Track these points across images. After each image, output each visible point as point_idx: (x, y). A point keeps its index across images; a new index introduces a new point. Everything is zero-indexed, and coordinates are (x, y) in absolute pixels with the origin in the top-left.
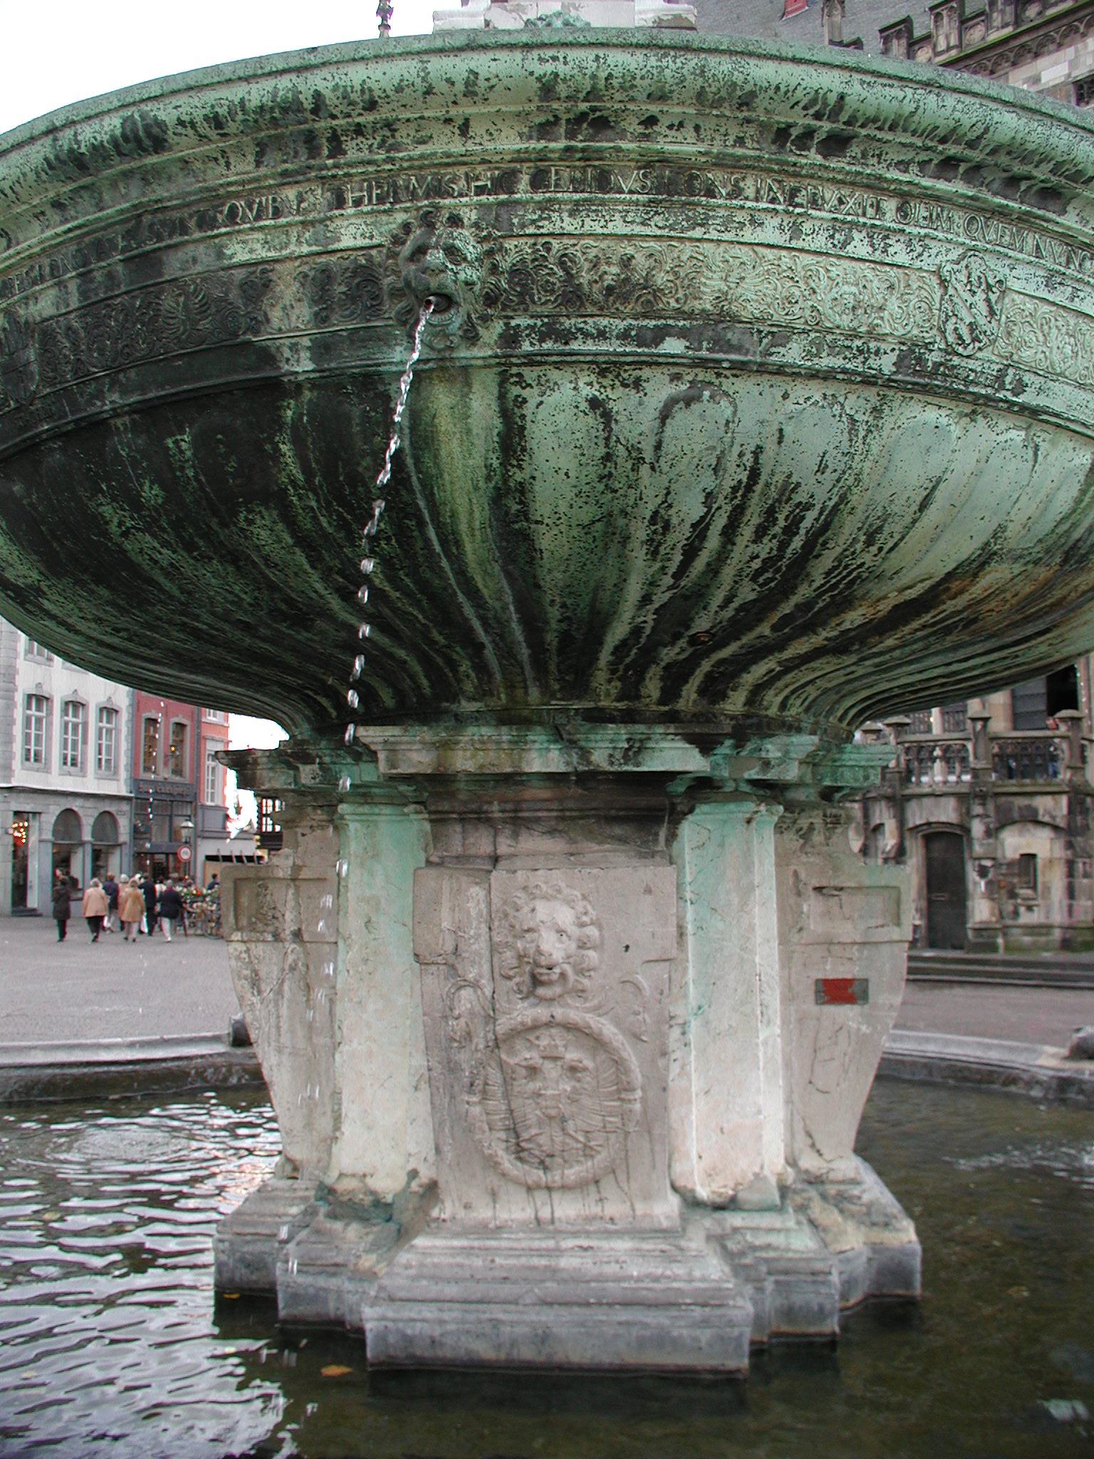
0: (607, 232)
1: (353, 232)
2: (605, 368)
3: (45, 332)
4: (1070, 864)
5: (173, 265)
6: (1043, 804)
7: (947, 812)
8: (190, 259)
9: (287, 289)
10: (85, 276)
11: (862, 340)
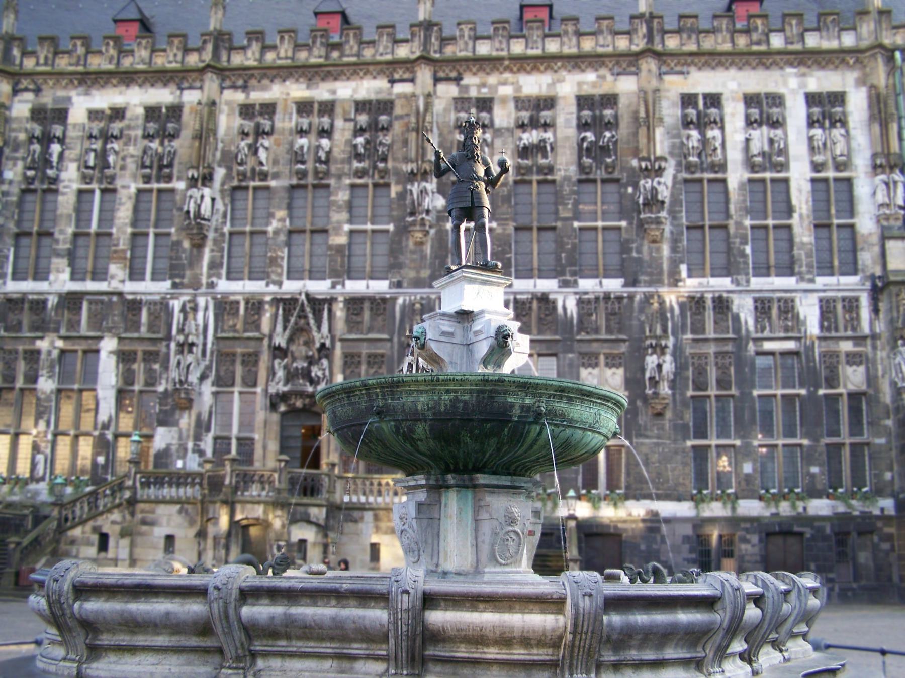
0: (560, 406)
2: (555, 425)
3: (465, 402)
4: (326, 547)
8: (500, 399)
9: (517, 407)
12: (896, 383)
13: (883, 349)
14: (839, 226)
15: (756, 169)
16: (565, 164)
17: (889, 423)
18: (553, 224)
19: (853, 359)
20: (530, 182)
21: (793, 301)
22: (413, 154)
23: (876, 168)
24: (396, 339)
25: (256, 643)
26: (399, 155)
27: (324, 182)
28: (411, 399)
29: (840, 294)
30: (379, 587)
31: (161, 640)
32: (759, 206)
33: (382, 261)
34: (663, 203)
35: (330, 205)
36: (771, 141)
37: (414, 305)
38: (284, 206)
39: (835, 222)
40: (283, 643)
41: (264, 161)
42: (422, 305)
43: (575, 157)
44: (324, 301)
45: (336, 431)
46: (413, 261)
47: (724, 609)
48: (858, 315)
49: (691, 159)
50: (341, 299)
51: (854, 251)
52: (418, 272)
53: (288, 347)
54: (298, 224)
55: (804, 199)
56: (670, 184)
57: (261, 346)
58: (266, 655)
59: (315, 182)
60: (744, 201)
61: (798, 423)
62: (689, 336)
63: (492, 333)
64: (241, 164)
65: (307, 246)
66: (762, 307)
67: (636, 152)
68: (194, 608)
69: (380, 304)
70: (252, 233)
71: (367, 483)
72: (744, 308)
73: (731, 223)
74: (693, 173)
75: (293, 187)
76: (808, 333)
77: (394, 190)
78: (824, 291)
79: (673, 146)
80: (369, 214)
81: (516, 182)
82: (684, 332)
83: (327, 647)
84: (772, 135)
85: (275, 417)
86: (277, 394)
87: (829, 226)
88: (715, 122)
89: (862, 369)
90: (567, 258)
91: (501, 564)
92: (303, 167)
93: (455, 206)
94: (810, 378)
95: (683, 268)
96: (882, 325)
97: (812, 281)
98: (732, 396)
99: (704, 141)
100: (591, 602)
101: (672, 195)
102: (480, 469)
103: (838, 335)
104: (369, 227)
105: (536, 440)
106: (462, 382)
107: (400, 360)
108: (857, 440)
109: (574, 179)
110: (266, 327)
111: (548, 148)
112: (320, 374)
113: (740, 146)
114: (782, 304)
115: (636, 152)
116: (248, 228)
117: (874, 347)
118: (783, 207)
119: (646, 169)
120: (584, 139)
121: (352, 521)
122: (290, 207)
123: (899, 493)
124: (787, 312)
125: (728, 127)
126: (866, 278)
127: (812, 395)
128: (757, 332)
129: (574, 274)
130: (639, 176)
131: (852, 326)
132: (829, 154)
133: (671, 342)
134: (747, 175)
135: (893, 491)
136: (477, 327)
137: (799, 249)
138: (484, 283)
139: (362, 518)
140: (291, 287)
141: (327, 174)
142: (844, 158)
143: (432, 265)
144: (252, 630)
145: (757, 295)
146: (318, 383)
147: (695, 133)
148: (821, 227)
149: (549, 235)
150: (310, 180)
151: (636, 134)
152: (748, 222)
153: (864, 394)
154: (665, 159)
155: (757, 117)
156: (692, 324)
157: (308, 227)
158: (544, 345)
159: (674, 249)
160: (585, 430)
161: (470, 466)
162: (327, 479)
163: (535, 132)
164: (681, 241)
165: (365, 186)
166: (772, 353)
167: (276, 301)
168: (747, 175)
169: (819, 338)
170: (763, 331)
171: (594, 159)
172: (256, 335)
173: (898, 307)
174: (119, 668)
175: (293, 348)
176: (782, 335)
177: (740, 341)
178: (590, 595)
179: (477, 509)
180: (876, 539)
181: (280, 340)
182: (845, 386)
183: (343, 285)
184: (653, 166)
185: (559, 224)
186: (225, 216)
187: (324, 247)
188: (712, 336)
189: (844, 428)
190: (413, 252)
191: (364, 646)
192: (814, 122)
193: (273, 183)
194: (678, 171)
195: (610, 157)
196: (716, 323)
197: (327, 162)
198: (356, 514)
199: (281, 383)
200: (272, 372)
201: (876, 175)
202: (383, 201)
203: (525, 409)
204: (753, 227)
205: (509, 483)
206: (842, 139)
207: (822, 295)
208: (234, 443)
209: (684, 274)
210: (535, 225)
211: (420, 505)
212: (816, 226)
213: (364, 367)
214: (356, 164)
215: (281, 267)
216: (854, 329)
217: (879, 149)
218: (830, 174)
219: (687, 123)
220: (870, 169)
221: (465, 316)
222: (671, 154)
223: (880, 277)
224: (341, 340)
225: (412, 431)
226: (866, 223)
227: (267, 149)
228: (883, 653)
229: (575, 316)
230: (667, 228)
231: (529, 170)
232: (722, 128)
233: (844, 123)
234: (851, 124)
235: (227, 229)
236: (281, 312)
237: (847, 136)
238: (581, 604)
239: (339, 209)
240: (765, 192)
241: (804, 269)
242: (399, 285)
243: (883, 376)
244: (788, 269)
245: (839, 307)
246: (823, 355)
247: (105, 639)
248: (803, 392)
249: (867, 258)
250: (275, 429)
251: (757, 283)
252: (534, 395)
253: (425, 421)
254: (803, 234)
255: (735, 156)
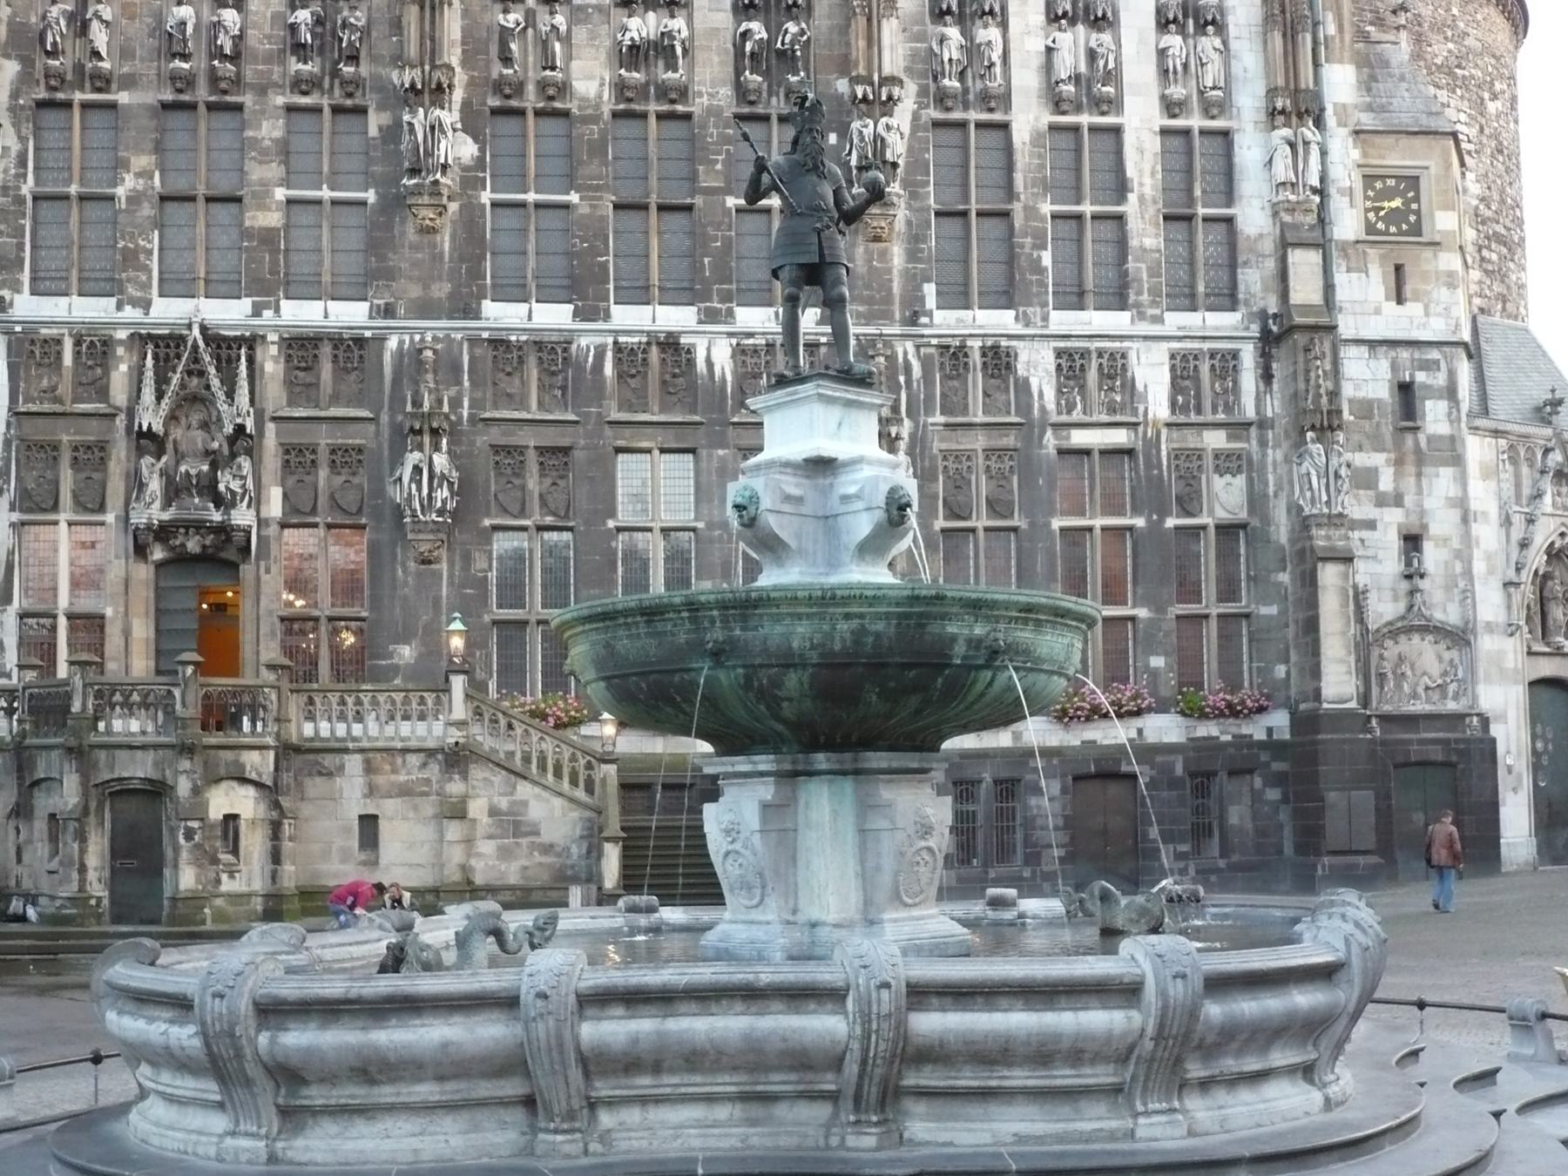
0: (1024, 635)
1: (978, 630)
3: (878, 635)
5: (929, 629)
6: (251, 759)
7: (139, 768)
8: (934, 628)
9: (961, 641)
10: (899, 624)
11: (1052, 661)
12: (1300, 509)
13: (1276, 446)
14: (1206, 219)
15: (1065, 107)
16: (710, 84)
17: (1284, 578)
18: (688, 201)
19: (1228, 463)
20: (643, 116)
21: (1124, 356)
22: (413, 51)
23: (1273, 115)
24: (385, 418)
25: (598, 1084)
26: (385, 48)
27: (228, 98)
28: (779, 629)
29: (1206, 346)
30: (827, 977)
31: (426, 1091)
32: (1067, 178)
33: (353, 264)
34: (895, 165)
35: (243, 147)
36: (1092, 55)
37: (420, 351)
38: (151, 146)
39: (1202, 211)
40: (645, 1080)
41: (104, 54)
42: (435, 352)
43: (731, 69)
44: (240, 341)
45: (606, 679)
46: (416, 264)
47: (1350, 982)
48: (1235, 382)
49: (946, 82)
50: (273, 337)
51: (1233, 266)
52: (426, 287)
53: (166, 434)
54: (180, 185)
55: (1147, 168)
56: (906, 130)
57: (111, 430)
58: (612, 1103)
59: (213, 98)
60: (1042, 166)
61: (1129, 578)
62: (939, 418)
63: (881, 500)
64: (52, 54)
65: (201, 228)
66: (1071, 365)
67: (844, 66)
68: (489, 1032)
69: (353, 350)
70: (82, 198)
71: (350, 700)
72: (1037, 367)
73: (1017, 208)
74: (948, 109)
75: (166, 106)
76: (1150, 416)
77: (375, 122)
78: (1180, 339)
79: (914, 56)
80: (326, 169)
81: (616, 115)
82: (929, 411)
83: (726, 1083)
84: (1093, 44)
85: (144, 572)
86: (149, 527)
87: (1189, 218)
88: (991, 12)
89: (1240, 481)
90: (713, 265)
91: (906, 905)
92: (186, 66)
93: (788, 260)
94: (1152, 498)
95: (930, 290)
96: (1276, 403)
97: (1159, 320)
98: (1015, 529)
99: (973, 50)
100: (1186, 987)
101: (910, 150)
102: (869, 742)
103: (1201, 419)
104: (326, 193)
105: (982, 695)
106: (875, 600)
107: (397, 459)
108: (1230, 608)
109: (728, 114)
110: (119, 393)
111: (679, 50)
112: (235, 485)
113: (1037, 61)
114: (1104, 361)
115: (844, 66)
116: (74, 189)
117: (1263, 443)
118: (1109, 178)
119: (865, 99)
120: (746, 35)
121: (320, 774)
122: (159, 148)
123: (1297, 703)
124: (1112, 377)
125: (1013, 22)
126: (1251, 317)
127: (1155, 527)
128: (1060, 413)
129: (727, 297)
130: (849, 113)
131: (1226, 405)
132: (1194, 82)
133: (906, 428)
134: (1048, 118)
135: (1289, 698)
136: (848, 484)
137: (1137, 260)
138: (849, 404)
139: (341, 768)
140: (168, 311)
141: (237, 82)
142: (1220, 93)
143: (453, 275)
144: (594, 1063)
145: (1062, 344)
146: (233, 504)
147: (953, 33)
148: (1177, 218)
149: (677, 220)
150: (202, 94)
151: (844, 29)
152: (1047, 208)
153: (1244, 526)
154: (901, 83)
155: (1068, 7)
156: (943, 395)
157: (201, 190)
158: (671, 432)
159: (913, 255)
160: (1052, 673)
161: (854, 739)
162: (274, 697)
163: (651, 15)
164: (925, 239)
165: (317, 110)
166: (1087, 452)
167: (141, 340)
168: (1048, 118)
169: (1168, 425)
170: (1070, 408)
171: (766, 74)
172: (101, 407)
173: (1307, 371)
174: (350, 1145)
175: (177, 433)
176: (1105, 418)
177: (1029, 429)
178: (1184, 976)
179: (865, 807)
180: (1258, 782)
181: (151, 418)
182: (1211, 512)
183: (277, 310)
184: (877, 94)
185: (698, 201)
186: (22, 161)
187: (234, 233)
188: (980, 418)
189: (1209, 589)
190: (415, 247)
191: (793, 1077)
192: (1168, 22)
193: (123, 98)
194: (922, 106)
195: (796, 73)
196: (986, 394)
197: (235, 58)
198: (329, 761)
199: (157, 504)
200: (136, 484)
201: (1274, 128)
202: (355, 142)
203: (974, 643)
204: (1055, 217)
205: (915, 765)
206: (1216, 56)
207: (1176, 345)
208: (62, 622)
209: (931, 302)
210: (653, 200)
211: (765, 807)
212: (1166, 218)
213: (323, 473)
214: (295, 66)
215: (149, 271)
216: (1228, 409)
217: (1281, 82)
218: (1195, 122)
219: (940, 15)
220: (1263, 117)
221: (821, 466)
222: (908, 70)
223: (1275, 316)
224: (274, 419)
225: (776, 683)
226: (1253, 217)
227: (107, 24)
228: (1421, 1005)
229: (729, 378)
230: (901, 214)
231: (642, 91)
232: (1004, 25)
233: (1220, 27)
234: (1232, 31)
235: (28, 187)
236: (149, 362)
237: (1225, 51)
238: (1171, 992)
239: (264, 157)
240: (1078, 151)
241: (1145, 297)
242: (388, 312)
243: (1276, 496)
244: (1118, 298)
245: (1205, 368)
246: (1176, 455)
247: (316, 1095)
248: (1140, 522)
249: (1254, 280)
250: (143, 595)
251: (1063, 321)
252: (988, 618)
253: (804, 666)
254: (1146, 235)
255: (1025, 80)
